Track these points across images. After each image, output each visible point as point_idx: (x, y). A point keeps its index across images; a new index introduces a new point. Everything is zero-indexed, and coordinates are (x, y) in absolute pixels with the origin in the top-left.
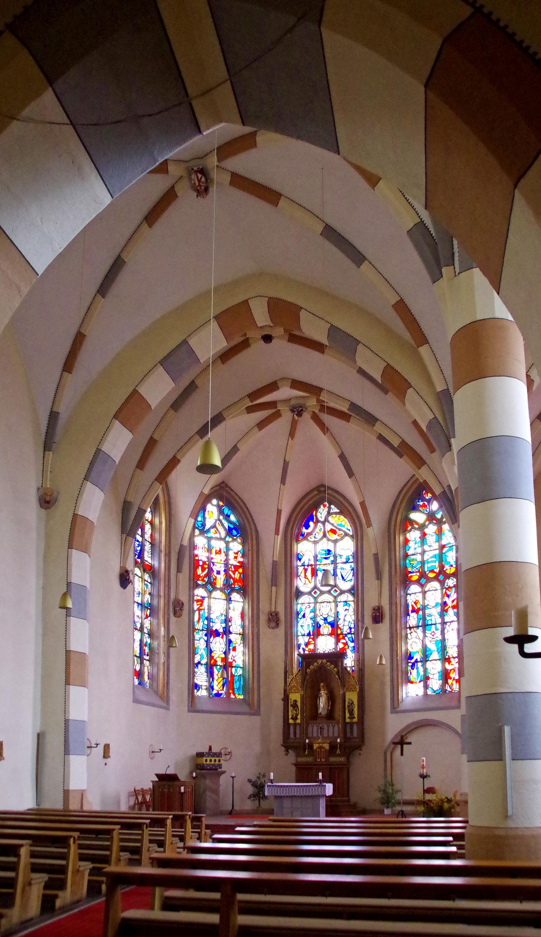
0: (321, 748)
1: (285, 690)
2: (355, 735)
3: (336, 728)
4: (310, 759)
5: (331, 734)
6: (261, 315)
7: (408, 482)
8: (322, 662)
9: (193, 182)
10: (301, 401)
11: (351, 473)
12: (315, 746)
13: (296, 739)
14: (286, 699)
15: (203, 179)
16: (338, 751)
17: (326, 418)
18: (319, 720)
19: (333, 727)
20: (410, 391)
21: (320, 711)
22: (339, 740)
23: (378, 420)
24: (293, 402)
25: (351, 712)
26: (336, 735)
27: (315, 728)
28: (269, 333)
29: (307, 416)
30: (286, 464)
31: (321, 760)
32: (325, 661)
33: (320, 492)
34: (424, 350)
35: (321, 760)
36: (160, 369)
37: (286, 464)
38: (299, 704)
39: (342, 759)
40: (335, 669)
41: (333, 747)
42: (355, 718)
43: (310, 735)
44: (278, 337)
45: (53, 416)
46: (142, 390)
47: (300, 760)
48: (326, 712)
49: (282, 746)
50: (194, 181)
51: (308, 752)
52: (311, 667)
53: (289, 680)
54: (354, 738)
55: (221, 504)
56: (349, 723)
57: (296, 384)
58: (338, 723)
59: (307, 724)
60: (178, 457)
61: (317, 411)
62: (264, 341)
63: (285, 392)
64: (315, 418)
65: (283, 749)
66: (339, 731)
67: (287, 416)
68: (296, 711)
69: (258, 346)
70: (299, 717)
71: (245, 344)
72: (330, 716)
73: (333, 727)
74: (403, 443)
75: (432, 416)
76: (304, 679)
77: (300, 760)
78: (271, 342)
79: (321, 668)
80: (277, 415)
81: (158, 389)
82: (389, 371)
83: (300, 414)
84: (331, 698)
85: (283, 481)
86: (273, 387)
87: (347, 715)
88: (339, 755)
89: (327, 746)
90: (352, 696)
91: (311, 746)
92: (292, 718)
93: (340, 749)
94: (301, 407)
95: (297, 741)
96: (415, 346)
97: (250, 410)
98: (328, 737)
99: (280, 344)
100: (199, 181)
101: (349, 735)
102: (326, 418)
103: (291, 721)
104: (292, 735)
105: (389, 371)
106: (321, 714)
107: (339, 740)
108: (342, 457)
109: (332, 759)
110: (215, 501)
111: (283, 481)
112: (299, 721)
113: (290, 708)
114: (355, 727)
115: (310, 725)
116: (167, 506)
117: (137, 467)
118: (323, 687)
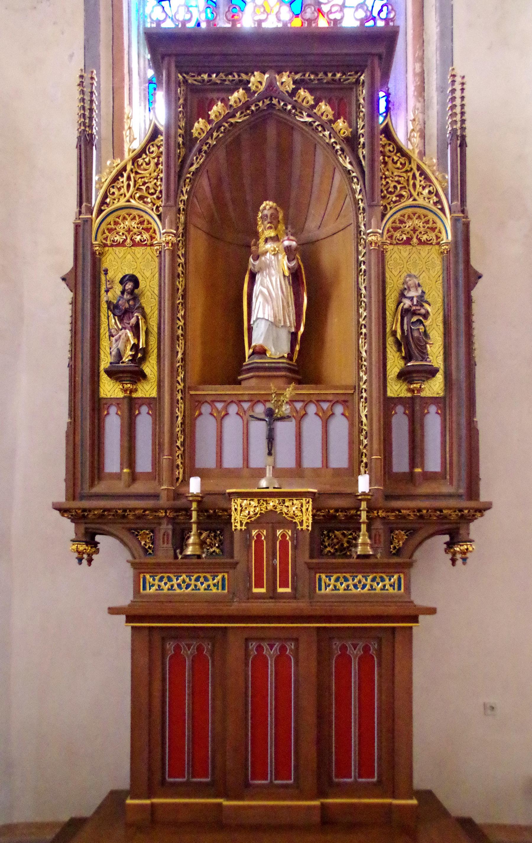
0: (270, 520)
1: (81, 230)
2: (433, 463)
3: (339, 426)
4: (209, 586)
5: (312, 459)
8: (271, 85)
12: (242, 512)
13: (134, 477)
14: (86, 274)
16: (363, 544)
18: (250, 385)
19: (326, 420)
21: (259, 337)
22: (364, 484)
25: (412, 346)
26: (339, 458)
27: (233, 425)
31: (272, 587)
32: (286, 81)
35: (272, 587)
38: (150, 301)
39: (385, 585)
40: (341, 124)
41: (334, 523)
42: (432, 372)
43: (205, 458)
47: (157, 586)
48: (285, 348)
49: (63, 511)
51: (202, 544)
52: (217, 109)
53: (99, 180)
54: (429, 477)
56: (400, 400)
58: (347, 399)
59: (196, 403)
65: (68, 528)
66: (353, 443)
68: (136, 330)
70: (150, 368)
72: (305, 364)
73: (326, 420)
76: (178, 171)
77: (157, 586)
79: (266, 118)
84: (309, 281)
87: (395, 364)
88: (365, 565)
89: (302, 513)
90: (420, 271)
91: (214, 517)
92: (110, 373)
93: (369, 530)
95: (139, 487)
98: (298, 471)
101: (401, 464)
103: (110, 389)
104: (113, 462)
106: (261, 352)
107: (364, 484)
109: (332, 586)
112: (147, 390)
113: (108, 321)
114: (433, 423)
115: (206, 409)
118: (274, 220)
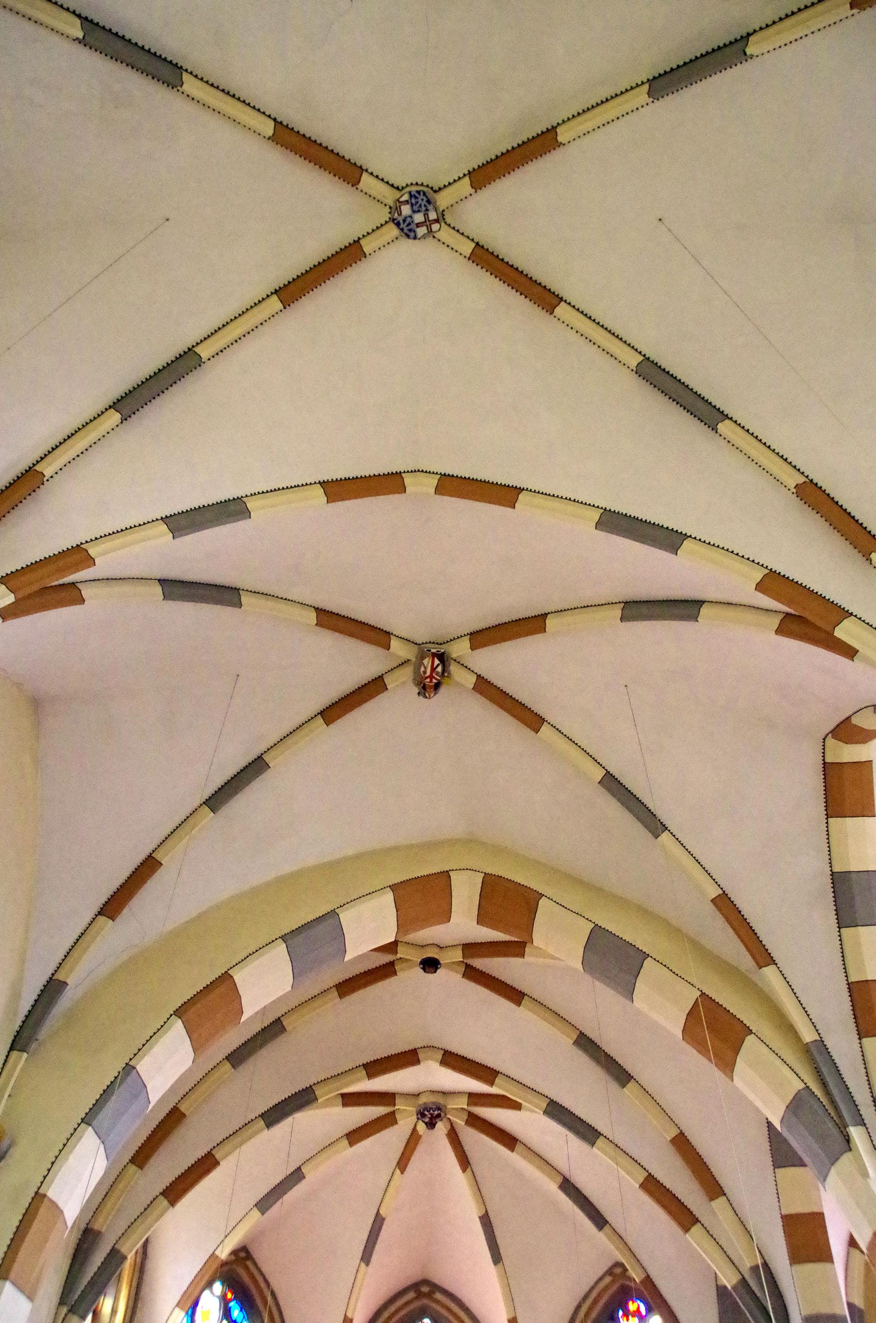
7: (592, 1289)
10: (440, 1100)
11: (497, 1258)
29: (441, 1127)
30: (379, 1221)
33: (420, 1295)
36: (281, 949)
37: (379, 1221)
45: (53, 988)
46: (238, 976)
55: (229, 1296)
60: (217, 1156)
64: (453, 1137)
80: (389, 1120)
81: (265, 984)
83: (431, 1125)
85: (366, 1257)
94: (439, 1109)
97: (350, 1099)
102: (472, 1138)
110: (218, 1287)
111: (366, 1257)
116: (136, 1275)
117: (133, 1161)
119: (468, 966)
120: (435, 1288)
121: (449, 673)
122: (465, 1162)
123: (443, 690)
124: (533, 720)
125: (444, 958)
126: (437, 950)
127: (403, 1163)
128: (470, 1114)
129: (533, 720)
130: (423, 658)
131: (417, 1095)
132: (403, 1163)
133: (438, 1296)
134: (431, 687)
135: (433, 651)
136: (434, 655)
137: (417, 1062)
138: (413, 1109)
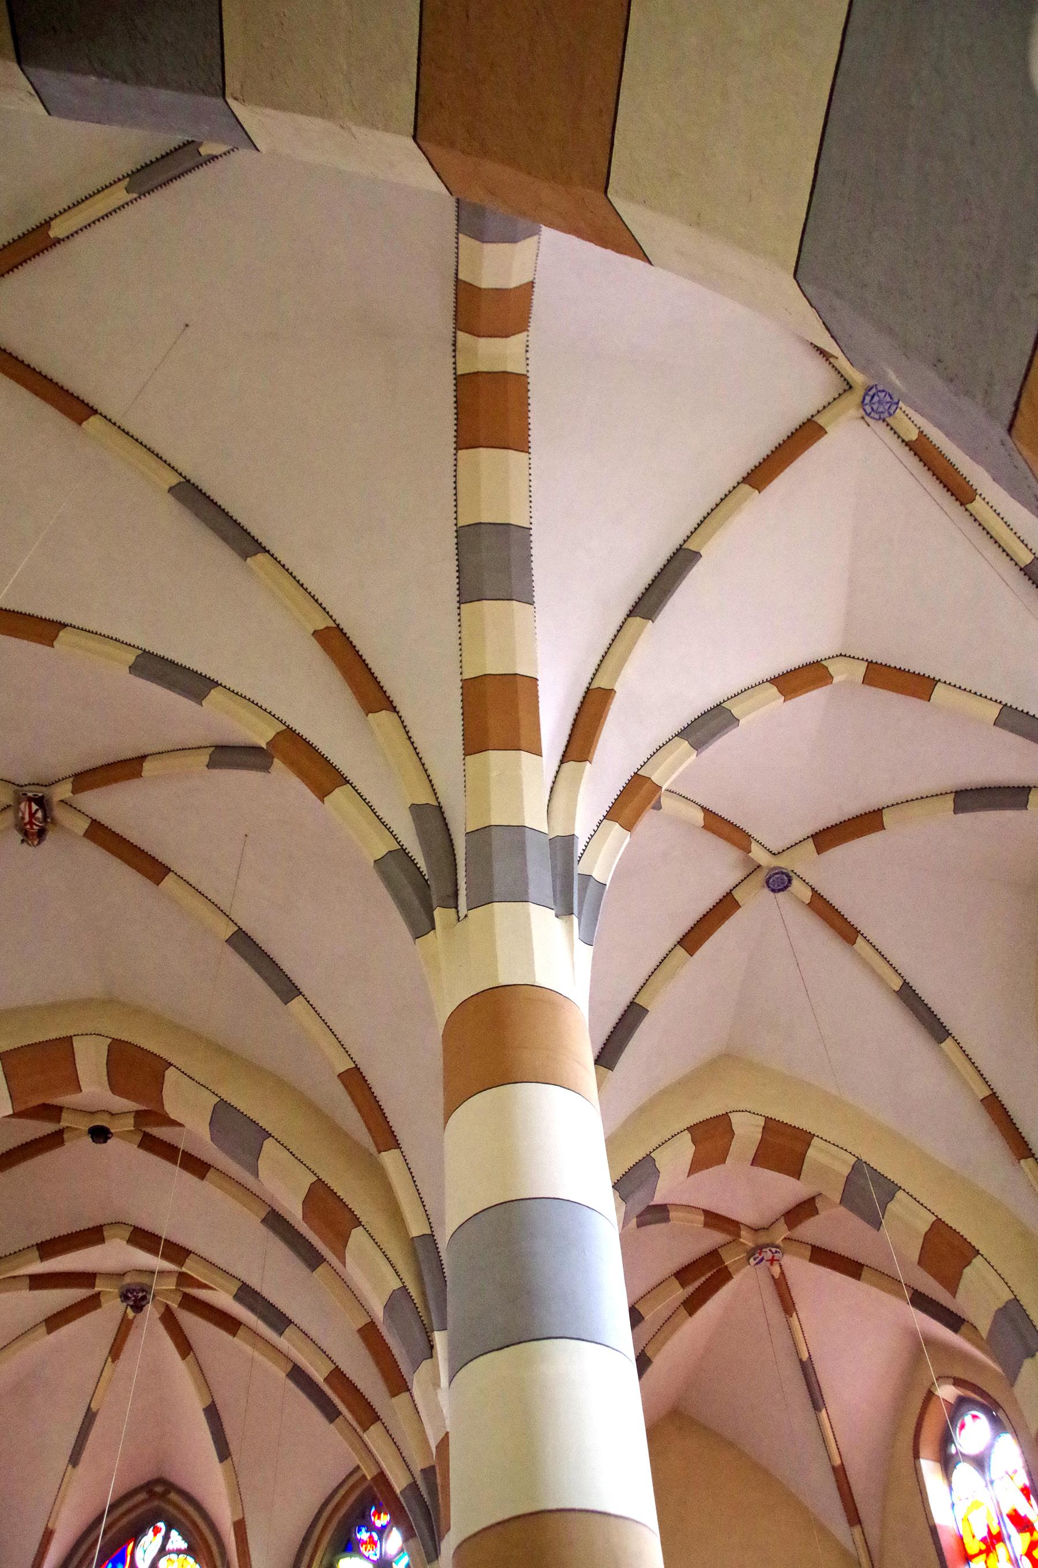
6: (93, 1085)
9: (20, 815)
10: (144, 1280)
11: (224, 1452)
15: (39, 815)
17: (189, 1320)
20: (357, 1233)
23: (290, 1322)
24: (128, 1280)
28: (104, 1124)
34: (389, 1159)
44: (123, 1136)
50: (24, 814)
57: (143, 1238)
61: (174, 1306)
62: (92, 1137)
63: (115, 1255)
64: (169, 1319)
67: (113, 1308)
69: (80, 1147)
71: (55, 1140)
74: (337, 1376)
75: (396, 1284)
78: (105, 1142)
82: (321, 1199)
83: (138, 1307)
86: (93, 1236)
94: (143, 1291)
96: (373, 1149)
99: (122, 1150)
100: (32, 815)
102: (189, 1320)
105: (321, 1199)
108: (212, 1413)
119: (146, 1135)
120: (170, 1486)
121: (54, 822)
122: (184, 1346)
123: (50, 836)
124: (153, 868)
125: (115, 1127)
126: (106, 1117)
127: (115, 1352)
128: (186, 1296)
129: (153, 868)
130: (20, 803)
131: (122, 1275)
132: (115, 1352)
133: (173, 1496)
134: (33, 834)
135: (30, 794)
136: (30, 800)
137: (102, 1240)
138: (116, 1291)
